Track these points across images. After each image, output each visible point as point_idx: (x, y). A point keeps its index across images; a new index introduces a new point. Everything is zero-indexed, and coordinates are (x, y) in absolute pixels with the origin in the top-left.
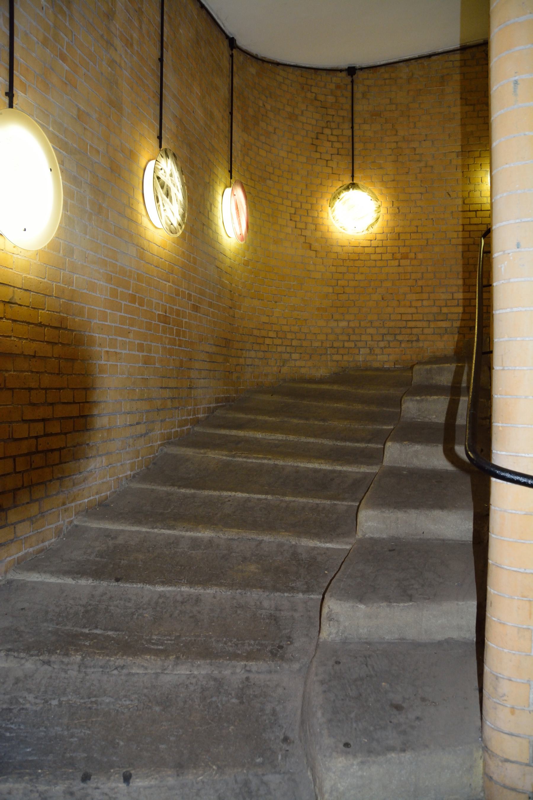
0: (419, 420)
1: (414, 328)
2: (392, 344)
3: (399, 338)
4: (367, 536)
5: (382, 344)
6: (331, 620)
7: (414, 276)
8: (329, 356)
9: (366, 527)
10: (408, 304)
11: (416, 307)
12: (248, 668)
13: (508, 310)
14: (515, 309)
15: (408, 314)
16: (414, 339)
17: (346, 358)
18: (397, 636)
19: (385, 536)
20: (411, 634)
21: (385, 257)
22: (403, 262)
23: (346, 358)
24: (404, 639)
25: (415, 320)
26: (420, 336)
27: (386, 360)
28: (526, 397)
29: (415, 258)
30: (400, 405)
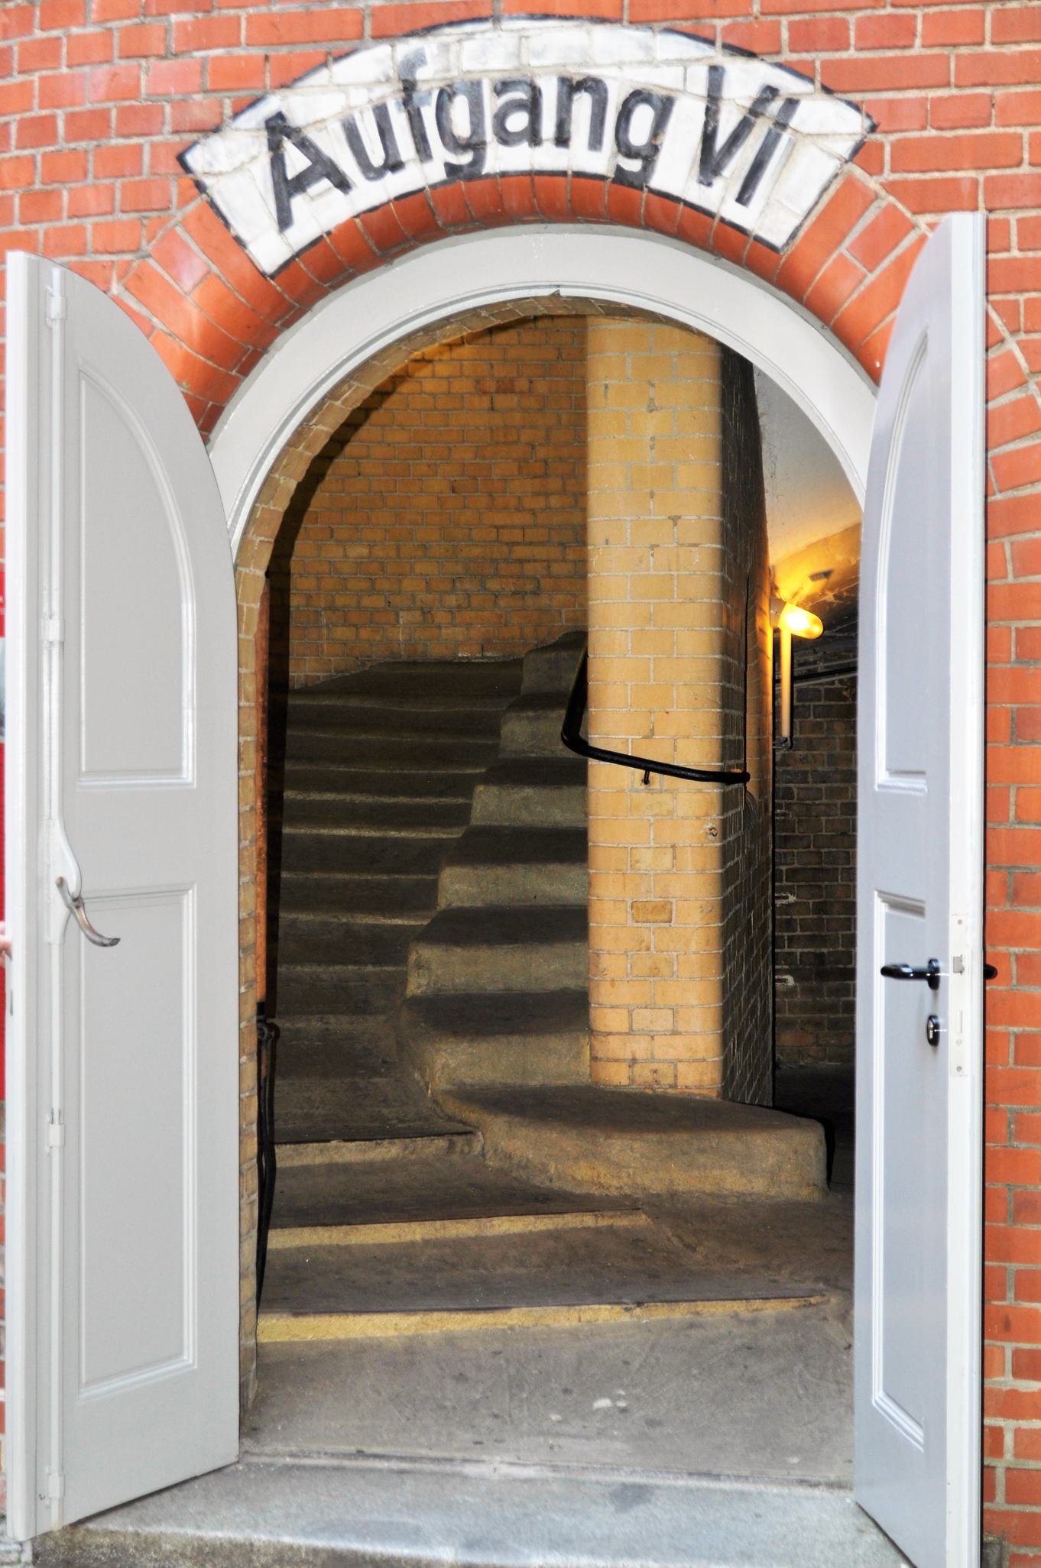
0: (532, 755)
1: (529, 561)
2: (476, 601)
3: (493, 585)
4: (454, 905)
5: (452, 601)
6: (420, 969)
7: (526, 436)
8: (325, 631)
9: (451, 892)
10: (513, 502)
11: (533, 512)
12: (325, 1020)
13: (599, 602)
14: (604, 601)
15: (513, 527)
16: (529, 587)
17: (365, 634)
18: (501, 986)
19: (479, 904)
20: (532, 1218)
21: (458, 386)
22: (502, 401)
23: (365, 634)
24: (509, 990)
25: (531, 544)
26: (542, 581)
27: (460, 638)
28: (615, 683)
29: (530, 390)
30: (495, 732)
